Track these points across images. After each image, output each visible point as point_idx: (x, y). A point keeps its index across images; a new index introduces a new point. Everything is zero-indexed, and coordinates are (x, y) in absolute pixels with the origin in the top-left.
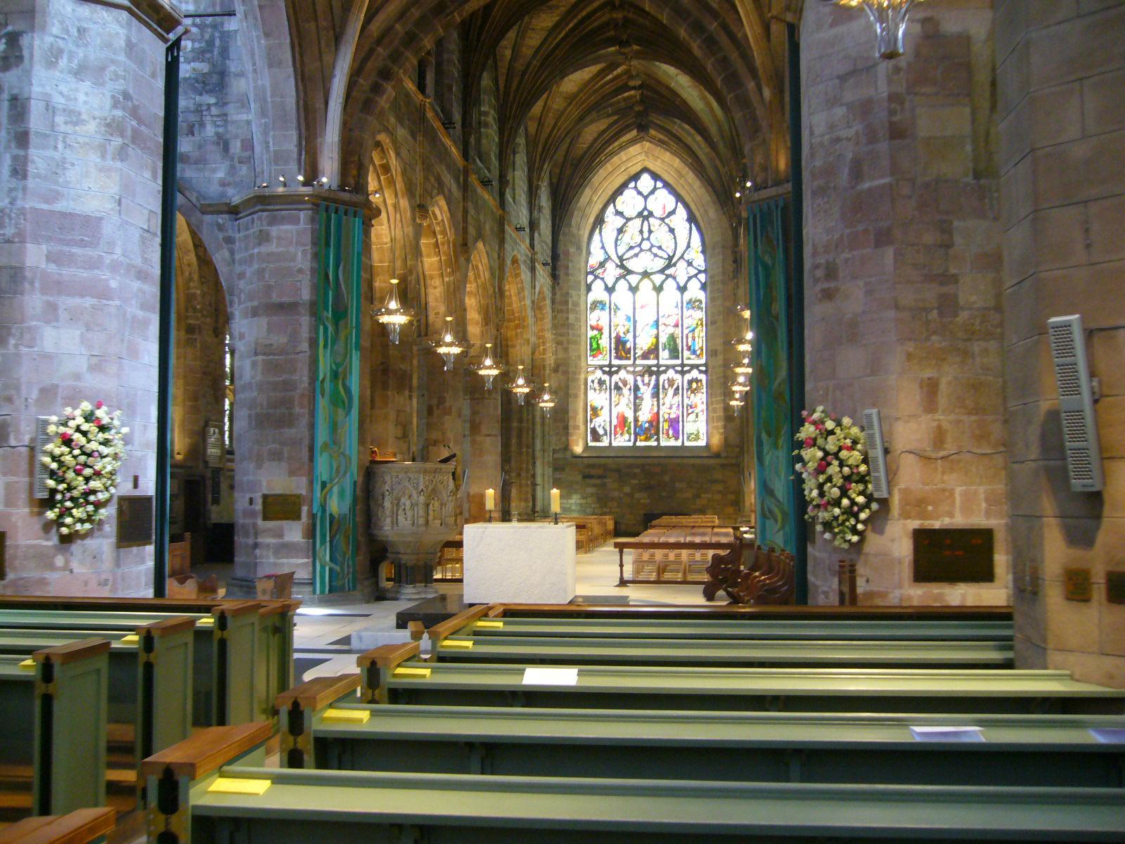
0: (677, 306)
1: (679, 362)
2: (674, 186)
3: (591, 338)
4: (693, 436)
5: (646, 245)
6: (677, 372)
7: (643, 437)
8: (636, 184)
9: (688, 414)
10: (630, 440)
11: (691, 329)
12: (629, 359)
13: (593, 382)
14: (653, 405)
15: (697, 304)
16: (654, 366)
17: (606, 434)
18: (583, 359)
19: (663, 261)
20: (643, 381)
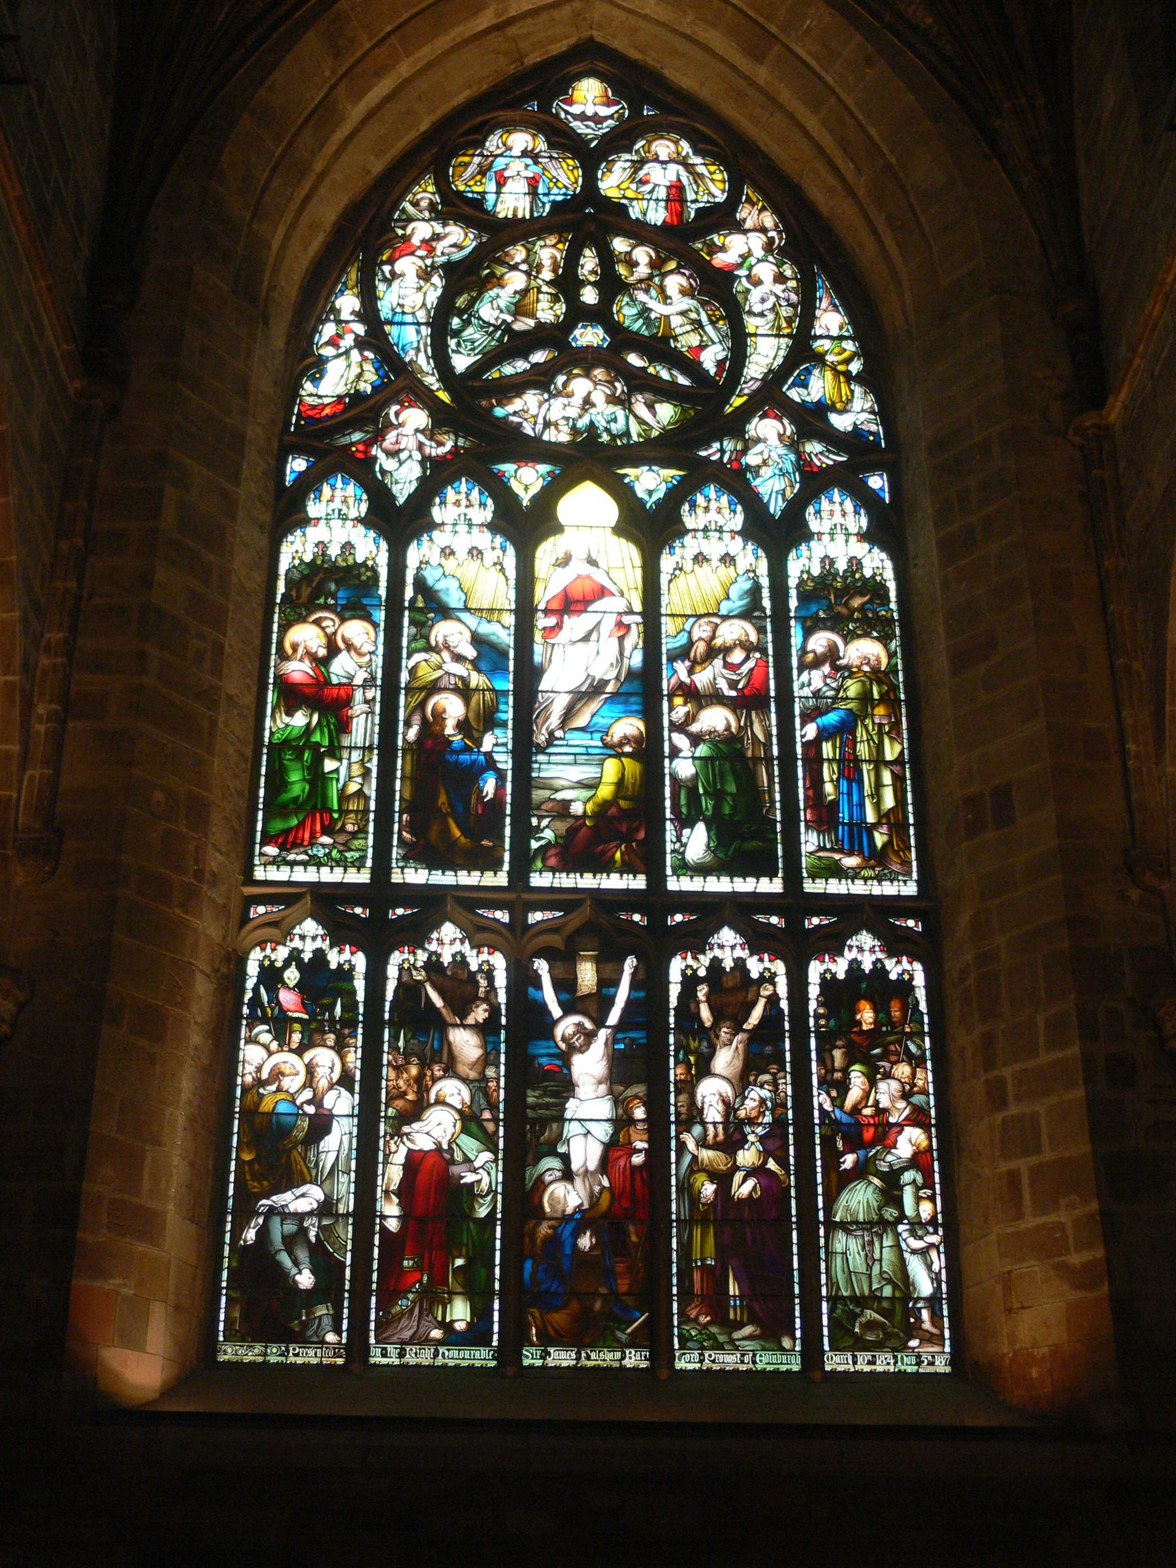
0: (750, 612)
1: (772, 886)
2: (729, 110)
3: (277, 749)
4: (870, 1314)
5: (589, 336)
6: (758, 941)
7: (559, 1318)
8: (545, 108)
9: (839, 1181)
10: (476, 1335)
11: (832, 718)
12: (495, 866)
13: (271, 976)
14: (621, 1122)
15: (857, 602)
16: (628, 899)
17: (328, 1287)
18: (219, 833)
19: (666, 412)
20: (565, 985)
